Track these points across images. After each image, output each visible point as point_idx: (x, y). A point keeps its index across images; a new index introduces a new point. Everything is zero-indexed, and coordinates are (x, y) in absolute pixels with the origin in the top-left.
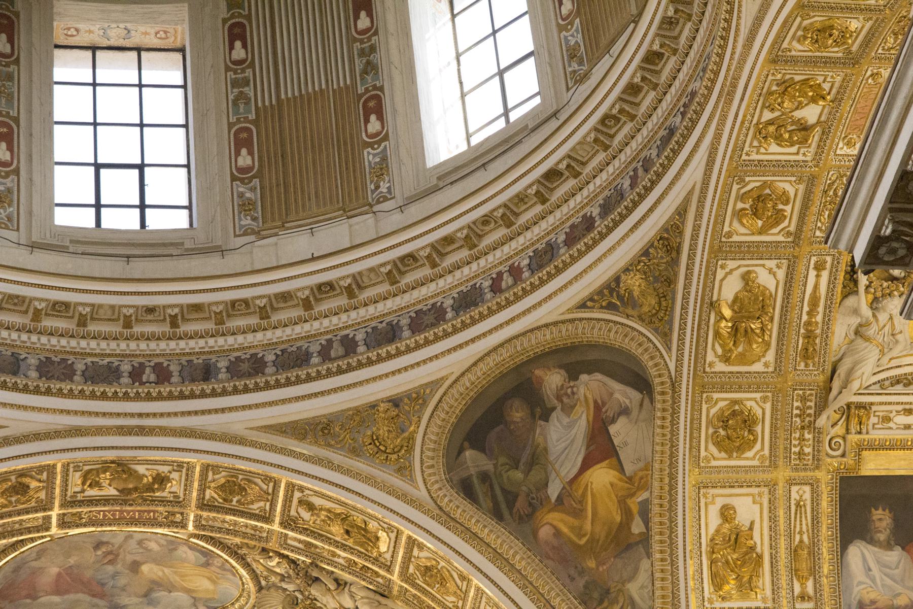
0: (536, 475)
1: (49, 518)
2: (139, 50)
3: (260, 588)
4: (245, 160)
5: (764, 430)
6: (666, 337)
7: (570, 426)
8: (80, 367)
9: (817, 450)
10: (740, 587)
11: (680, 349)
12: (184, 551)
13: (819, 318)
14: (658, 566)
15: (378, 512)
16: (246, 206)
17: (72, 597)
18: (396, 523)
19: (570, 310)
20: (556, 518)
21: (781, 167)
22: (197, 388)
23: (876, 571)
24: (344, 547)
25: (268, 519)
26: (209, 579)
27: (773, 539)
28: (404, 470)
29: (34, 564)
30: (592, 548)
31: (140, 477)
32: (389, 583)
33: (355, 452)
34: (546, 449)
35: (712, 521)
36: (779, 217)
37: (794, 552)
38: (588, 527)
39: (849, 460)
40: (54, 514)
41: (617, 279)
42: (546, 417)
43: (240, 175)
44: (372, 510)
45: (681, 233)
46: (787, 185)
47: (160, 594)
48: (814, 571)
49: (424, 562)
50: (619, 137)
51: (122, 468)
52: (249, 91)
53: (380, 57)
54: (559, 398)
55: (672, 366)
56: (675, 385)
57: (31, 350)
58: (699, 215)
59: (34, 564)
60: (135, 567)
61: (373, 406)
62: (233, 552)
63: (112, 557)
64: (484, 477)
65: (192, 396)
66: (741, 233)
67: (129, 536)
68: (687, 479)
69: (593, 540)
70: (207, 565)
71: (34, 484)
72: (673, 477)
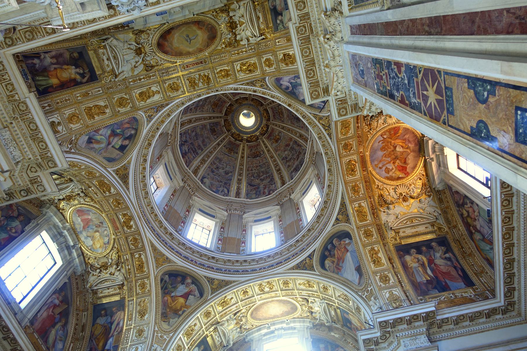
0: (172, 289)
3: (105, 256)
7: (185, 289)
13: (228, 313)
14: (179, 321)
15: (288, 277)
17: (81, 223)
19: (203, 275)
20: (169, 298)
26: (101, 246)
28: (157, 267)
29: (91, 213)
30: (171, 308)
33: (155, 257)
34: (177, 288)
38: (173, 305)
39: (209, 335)
41: (214, 279)
42: (183, 284)
48: (193, 346)
54: (187, 284)
59: (91, 213)
60: (98, 231)
61: (164, 255)
63: (98, 226)
64: (166, 281)
69: (172, 307)
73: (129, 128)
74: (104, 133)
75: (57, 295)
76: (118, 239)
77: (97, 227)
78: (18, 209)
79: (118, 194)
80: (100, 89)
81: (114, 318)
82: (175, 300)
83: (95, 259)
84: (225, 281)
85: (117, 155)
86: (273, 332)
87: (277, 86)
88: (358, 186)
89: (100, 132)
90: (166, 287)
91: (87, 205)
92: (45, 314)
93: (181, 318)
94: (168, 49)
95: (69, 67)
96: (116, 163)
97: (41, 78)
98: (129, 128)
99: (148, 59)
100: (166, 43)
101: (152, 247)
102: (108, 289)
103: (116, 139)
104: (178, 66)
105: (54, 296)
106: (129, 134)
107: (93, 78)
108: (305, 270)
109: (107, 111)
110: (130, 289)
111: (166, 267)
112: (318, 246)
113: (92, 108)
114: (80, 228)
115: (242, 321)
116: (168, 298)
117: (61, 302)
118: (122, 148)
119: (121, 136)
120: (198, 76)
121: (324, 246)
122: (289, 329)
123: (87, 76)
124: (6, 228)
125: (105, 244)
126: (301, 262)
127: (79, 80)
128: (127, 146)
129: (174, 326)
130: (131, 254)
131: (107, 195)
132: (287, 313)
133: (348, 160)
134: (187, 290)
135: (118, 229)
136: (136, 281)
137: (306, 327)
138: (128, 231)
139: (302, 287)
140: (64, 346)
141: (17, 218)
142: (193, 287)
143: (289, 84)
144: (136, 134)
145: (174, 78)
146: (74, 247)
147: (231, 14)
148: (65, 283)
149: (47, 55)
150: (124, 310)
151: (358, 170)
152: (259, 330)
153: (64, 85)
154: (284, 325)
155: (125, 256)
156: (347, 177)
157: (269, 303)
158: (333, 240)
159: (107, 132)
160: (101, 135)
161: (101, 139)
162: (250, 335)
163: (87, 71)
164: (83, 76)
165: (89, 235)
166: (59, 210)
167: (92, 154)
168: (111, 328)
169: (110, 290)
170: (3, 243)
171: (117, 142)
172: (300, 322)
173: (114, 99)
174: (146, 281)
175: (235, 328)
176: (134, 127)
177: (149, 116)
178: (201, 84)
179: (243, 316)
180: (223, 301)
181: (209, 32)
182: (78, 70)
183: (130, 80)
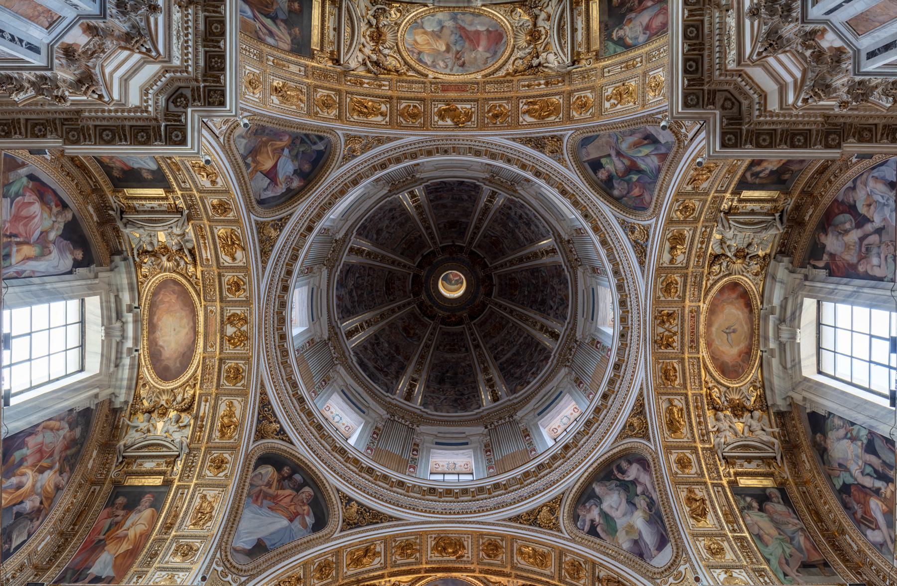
0: (295, 152)
12: (428, 60)
13: (201, 241)
17: (473, 29)
20: (282, 144)
29: (488, 55)
33: (367, 136)
42: (295, 172)
54: (292, 179)
59: (488, 55)
60: (448, 50)
61: (362, 153)
62: (410, 68)
63: (458, 56)
64: (315, 143)
69: (266, 146)
70: (419, 53)
73: (628, 193)
74: (648, 160)
76: (424, 83)
77: (458, 52)
79: (518, 125)
82: (274, 154)
83: (396, 24)
85: (588, 154)
86: (119, 316)
87: (628, 454)
88: (411, 555)
90: (305, 142)
91: (509, 58)
94: (726, 295)
98: (628, 193)
100: (734, 296)
102: (334, 29)
103: (620, 166)
104: (697, 304)
106: (616, 185)
108: (258, 419)
112: (300, 451)
114: (463, 21)
115: (168, 260)
118: (596, 165)
120: (674, 329)
121: (299, 466)
122: (119, 353)
125: (419, 53)
126: (273, 412)
128: (595, 173)
130: (391, 98)
131: (521, 105)
132: (155, 356)
133: (465, 543)
134: (281, 177)
135: (443, 90)
136: (339, 92)
137: (117, 391)
138: (436, 110)
139: (222, 409)
142: (281, 189)
143: (631, 478)
145: (684, 291)
147: (757, 414)
150: (293, 51)
151: (441, 558)
152: (131, 289)
154: (129, 344)
155: (387, 83)
156: (434, 536)
157: (191, 324)
158: (310, 486)
160: (647, 155)
161: (640, 151)
162: (128, 267)
165: (445, 30)
169: (332, 33)
171: (615, 165)
172: (130, 379)
174: (334, 112)
175: (155, 242)
177: (634, 228)
178: (660, 330)
179: (178, 265)
181: (733, 366)
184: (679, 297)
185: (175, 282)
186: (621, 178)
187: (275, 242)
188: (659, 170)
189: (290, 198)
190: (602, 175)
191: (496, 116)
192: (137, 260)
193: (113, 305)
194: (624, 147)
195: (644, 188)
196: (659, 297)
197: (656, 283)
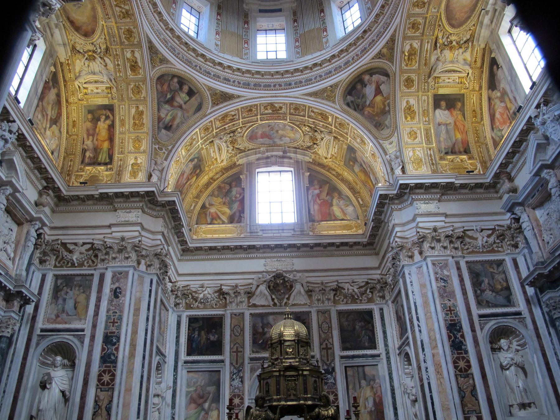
0: (363, 100)
1: (257, 118)
2: (275, 30)
4: (297, 44)
5: (416, 83)
6: (392, 63)
8: (262, 85)
9: (428, 87)
10: (411, 119)
11: (396, 65)
12: (287, 127)
16: (298, 53)
17: (264, 139)
18: (333, 113)
21: (418, 15)
22: (288, 87)
23: (442, 116)
24: (321, 121)
25: (304, 116)
27: (419, 110)
28: (334, 102)
31: (276, 107)
32: (332, 129)
33: (323, 99)
35: (404, 104)
36: (418, 28)
37: (424, 111)
38: (376, 110)
40: (259, 117)
41: (381, 51)
42: (365, 86)
43: (296, 47)
44: (327, 110)
45: (395, 36)
46: (420, 20)
47: (283, 138)
48: (428, 116)
49: (339, 122)
50: (380, 20)
51: (272, 105)
52: (298, 31)
53: (326, 21)
54: (368, 82)
55: (394, 70)
56: (395, 74)
57: (252, 82)
58: (399, 31)
60: (277, 131)
61: (326, 88)
63: (272, 129)
64: (352, 102)
65: (287, 89)
66: (410, 33)
67: (275, 123)
68: (398, 95)
70: (292, 130)
71: (254, 109)
72: (395, 95)
73: (169, 84)
74: (165, 112)
75: (312, 188)
78: (226, 183)
80: (121, 106)
81: (359, 161)
82: (374, 105)
84: (388, 41)
85: (196, 99)
89: (163, 116)
91: (245, 132)
92: (316, 207)
93: (391, 112)
94: (89, 28)
95: (98, 126)
96: (204, 103)
97: (100, 157)
98: (169, 84)
99: (99, 51)
100: (84, 28)
101: (311, 96)
103: (178, 99)
105: (310, 192)
106: (177, 85)
107: (110, 108)
109: (141, 108)
110: (341, 135)
111: (339, 93)
113: (134, 122)
115: (451, 42)
116: (367, 110)
117: (321, 187)
118: (191, 93)
119: (176, 93)
120: (118, 9)
123: (109, 113)
124: (232, 200)
127: (110, 123)
128: (190, 88)
129: (392, 124)
134: (374, 86)
140: (354, 206)
141: (231, 187)
142: (375, 77)
144: (178, 77)
145: (119, 33)
146: (285, 152)
148: (310, 176)
149: (85, 143)
152: (482, 23)
153: (111, 139)
159: (165, 109)
160: (167, 115)
161: (171, 115)
163: (104, 112)
164: (107, 118)
166: (245, 151)
167: (184, 127)
168: (364, 168)
170: (240, 209)
171: (181, 98)
173: (132, 98)
176: (170, 79)
178: (127, 7)
180: (406, 58)
182: (102, 120)
183: (118, 75)
184: (121, 29)
185: (453, 26)
186: (175, 91)
187: (385, 45)
188: (159, 110)
189: (371, 69)
190: (186, 88)
191: (251, 110)
192: (470, 44)
193: (495, 20)
194: (179, 113)
195: (162, 92)
196: (134, 28)
197: (139, 36)
